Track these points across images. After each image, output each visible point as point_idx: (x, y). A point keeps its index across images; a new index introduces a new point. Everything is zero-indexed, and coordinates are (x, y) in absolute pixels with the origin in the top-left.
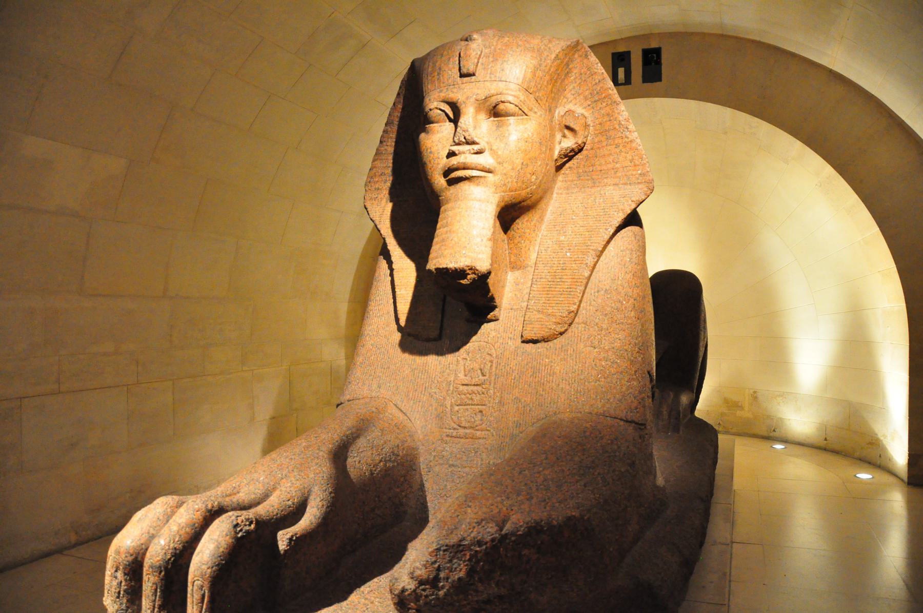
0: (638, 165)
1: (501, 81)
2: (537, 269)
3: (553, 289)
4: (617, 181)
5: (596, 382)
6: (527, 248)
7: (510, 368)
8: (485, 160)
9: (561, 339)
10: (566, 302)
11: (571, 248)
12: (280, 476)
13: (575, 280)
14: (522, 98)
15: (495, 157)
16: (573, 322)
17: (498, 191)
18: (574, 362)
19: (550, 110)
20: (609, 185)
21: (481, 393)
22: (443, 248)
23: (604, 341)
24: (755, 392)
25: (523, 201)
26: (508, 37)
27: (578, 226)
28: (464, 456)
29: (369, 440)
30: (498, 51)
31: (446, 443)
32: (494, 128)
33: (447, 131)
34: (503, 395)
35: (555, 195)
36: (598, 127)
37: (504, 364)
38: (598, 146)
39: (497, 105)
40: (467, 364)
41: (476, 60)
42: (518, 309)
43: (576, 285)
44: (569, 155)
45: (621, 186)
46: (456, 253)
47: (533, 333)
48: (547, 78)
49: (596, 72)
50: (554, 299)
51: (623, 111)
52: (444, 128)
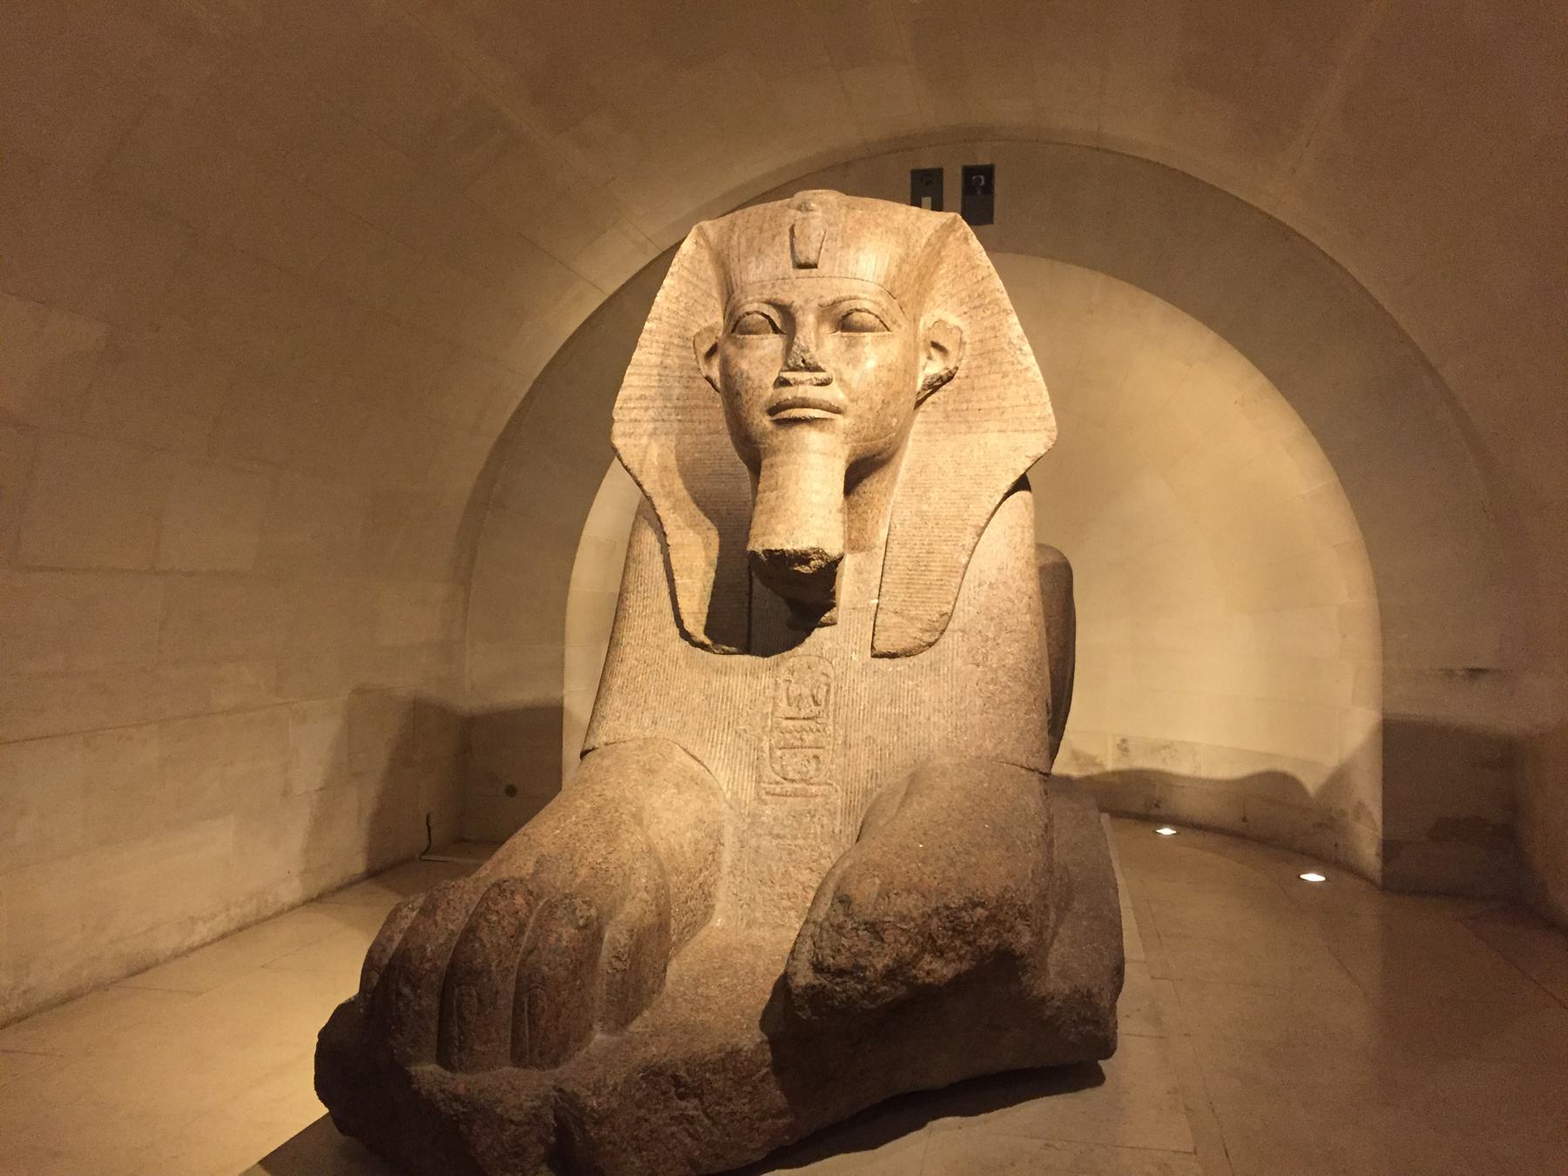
0: (1036, 405)
1: (855, 279)
2: (890, 552)
3: (915, 581)
5: (982, 714)
6: (875, 520)
7: (857, 693)
8: (834, 394)
9: (928, 655)
10: (937, 600)
11: (940, 522)
12: (582, 848)
13: (948, 569)
14: (885, 305)
15: (847, 391)
16: (946, 628)
18: (950, 687)
19: (915, 320)
20: (992, 432)
21: (814, 730)
22: (773, 521)
23: (990, 657)
24: (1124, 741)
25: (879, 455)
26: (861, 209)
27: (948, 489)
28: (794, 823)
29: (664, 799)
30: (850, 232)
31: (766, 804)
32: (843, 347)
33: (770, 348)
35: (910, 443)
36: (978, 345)
37: (847, 688)
38: (976, 373)
39: (849, 314)
40: (790, 689)
41: (819, 245)
42: (863, 608)
43: (950, 576)
44: (934, 386)
45: (1009, 433)
46: (794, 529)
47: (890, 643)
48: (915, 274)
49: (978, 265)
50: (919, 595)
51: (1015, 324)
52: (766, 342)
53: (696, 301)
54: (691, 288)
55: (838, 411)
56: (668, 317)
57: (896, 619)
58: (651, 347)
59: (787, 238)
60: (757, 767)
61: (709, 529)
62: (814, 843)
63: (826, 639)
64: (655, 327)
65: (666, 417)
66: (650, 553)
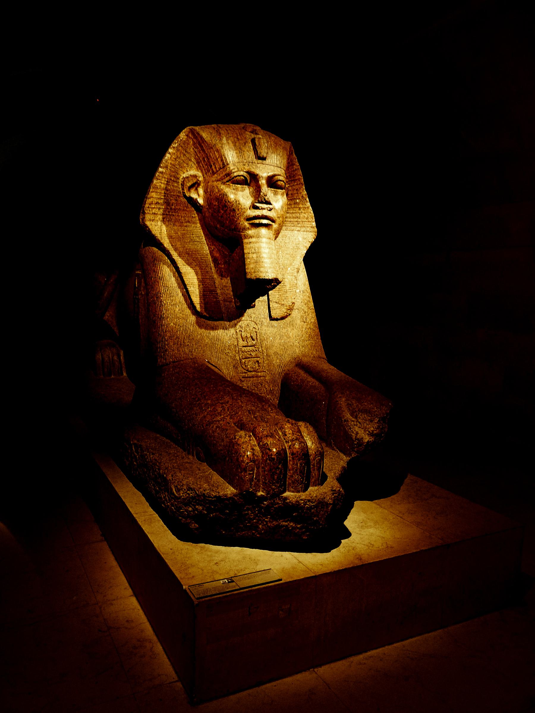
4: (298, 229)
17: (275, 233)
28: (256, 389)
34: (267, 351)
40: (242, 334)
45: (301, 232)
52: (243, 188)
53: (184, 162)
54: (182, 156)
55: (273, 221)
56: (171, 167)
57: (277, 305)
58: (162, 180)
59: (251, 145)
60: (236, 367)
61: (196, 266)
62: (264, 395)
63: (252, 313)
64: (164, 171)
65: (167, 213)
66: (169, 276)
